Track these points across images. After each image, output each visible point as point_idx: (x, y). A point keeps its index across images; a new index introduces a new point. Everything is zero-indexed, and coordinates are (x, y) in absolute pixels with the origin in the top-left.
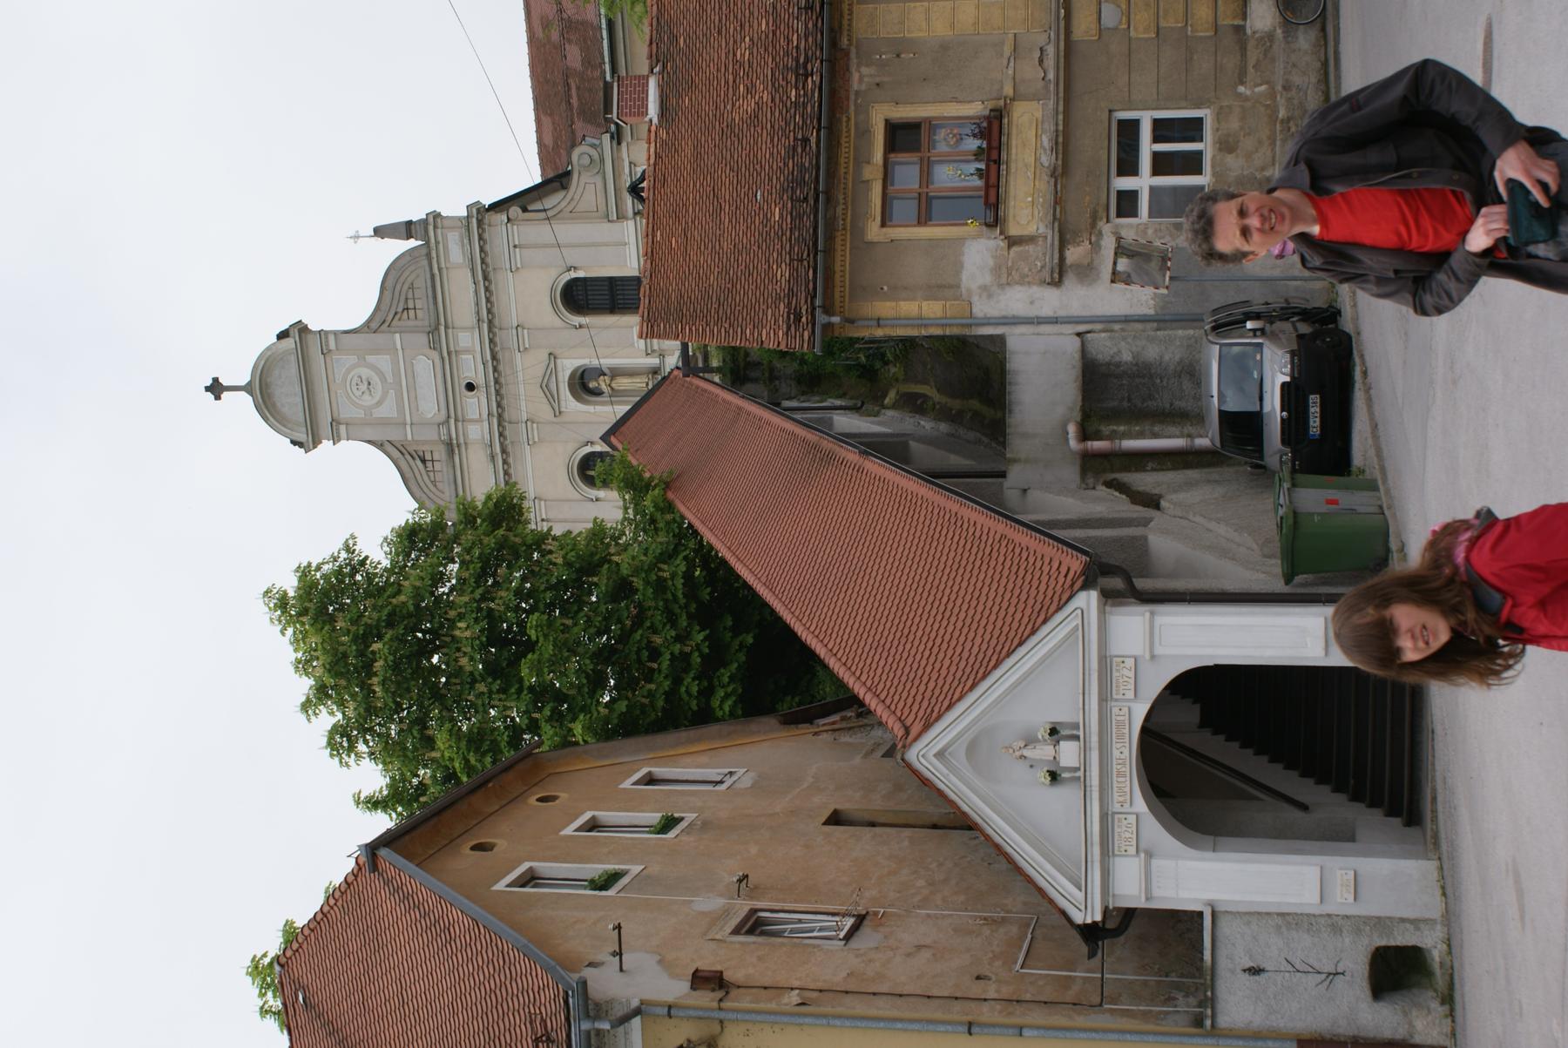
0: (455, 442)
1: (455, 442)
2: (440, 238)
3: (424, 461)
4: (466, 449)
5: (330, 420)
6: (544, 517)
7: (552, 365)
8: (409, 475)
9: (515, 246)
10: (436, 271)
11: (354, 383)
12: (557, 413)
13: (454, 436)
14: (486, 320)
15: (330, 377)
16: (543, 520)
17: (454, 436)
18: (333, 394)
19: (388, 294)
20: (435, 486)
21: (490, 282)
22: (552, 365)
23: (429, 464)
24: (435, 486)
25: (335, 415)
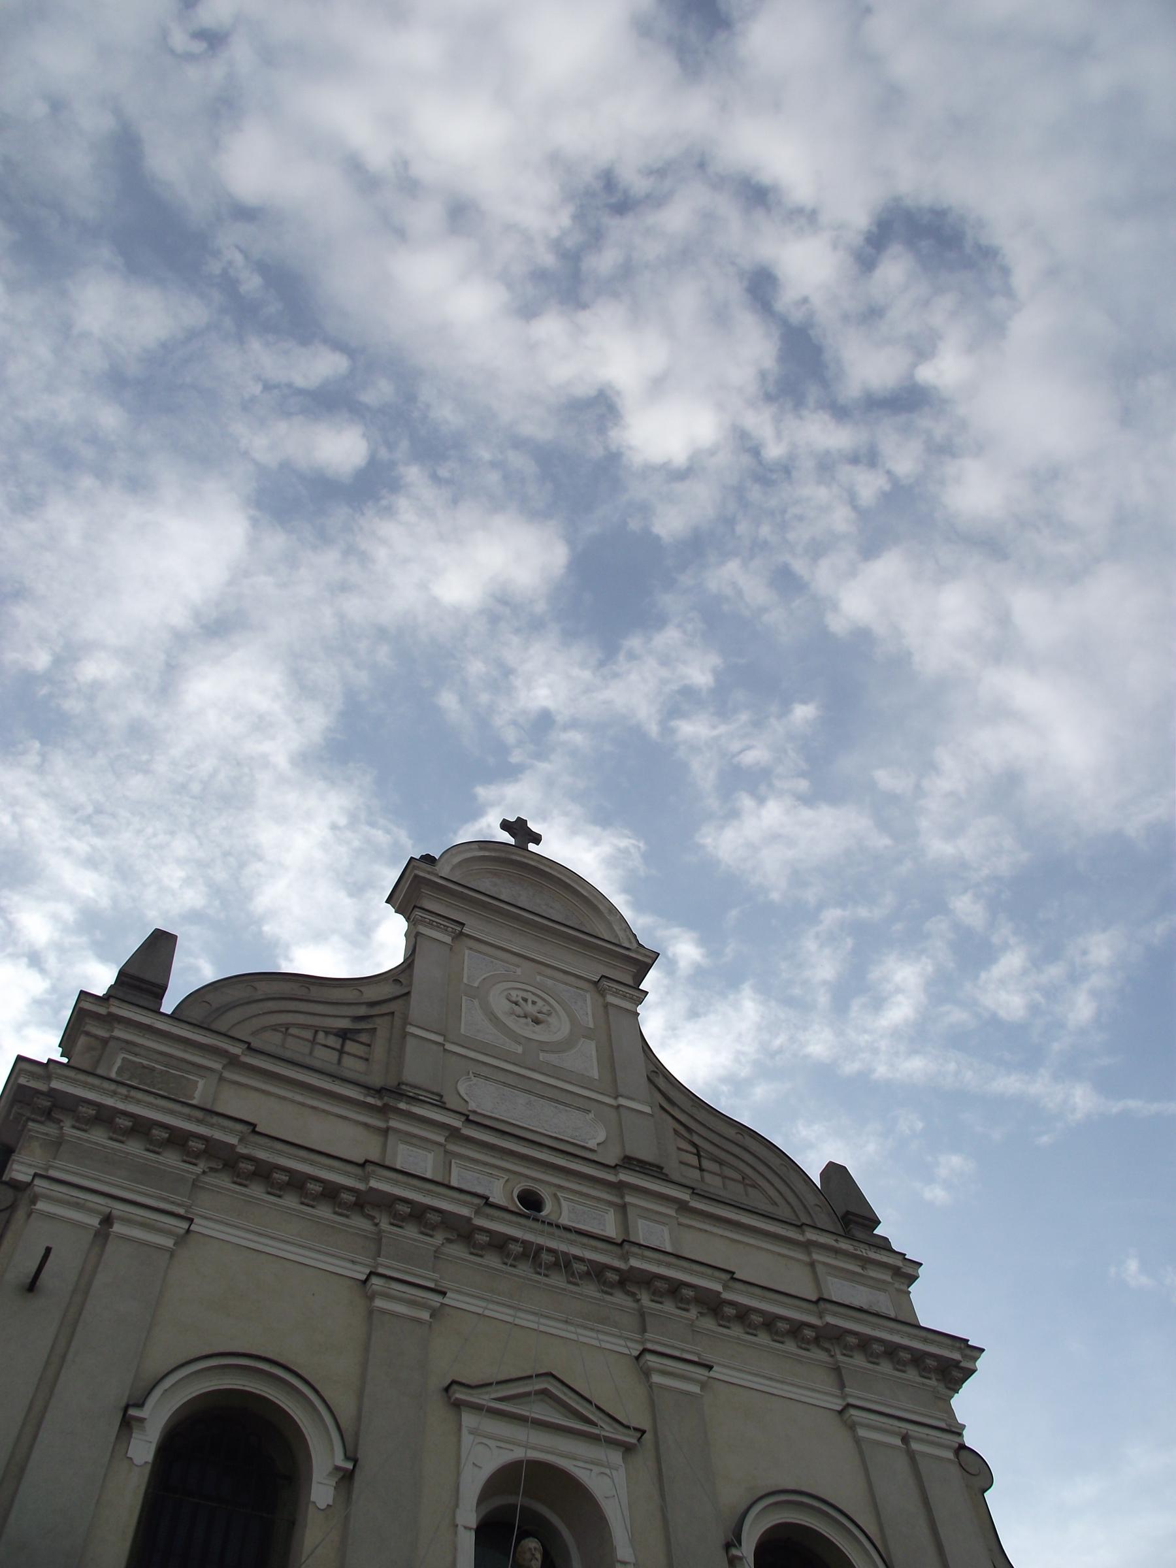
0: (402, 1106)
1: (402, 1106)
2: (872, 1273)
3: (344, 1035)
4: (366, 1126)
5: (466, 930)
6: (117, 1228)
7: (608, 1430)
8: (315, 992)
9: (905, 1439)
10: (811, 1235)
11: (531, 998)
12: (460, 1394)
13: (417, 1110)
14: (727, 1296)
15: (549, 972)
16: (107, 1220)
17: (417, 1110)
18: (515, 960)
19: (731, 1133)
20: (274, 1028)
21: (804, 1343)
22: (608, 1430)
23: (333, 1041)
24: (274, 1028)
25: (471, 943)
